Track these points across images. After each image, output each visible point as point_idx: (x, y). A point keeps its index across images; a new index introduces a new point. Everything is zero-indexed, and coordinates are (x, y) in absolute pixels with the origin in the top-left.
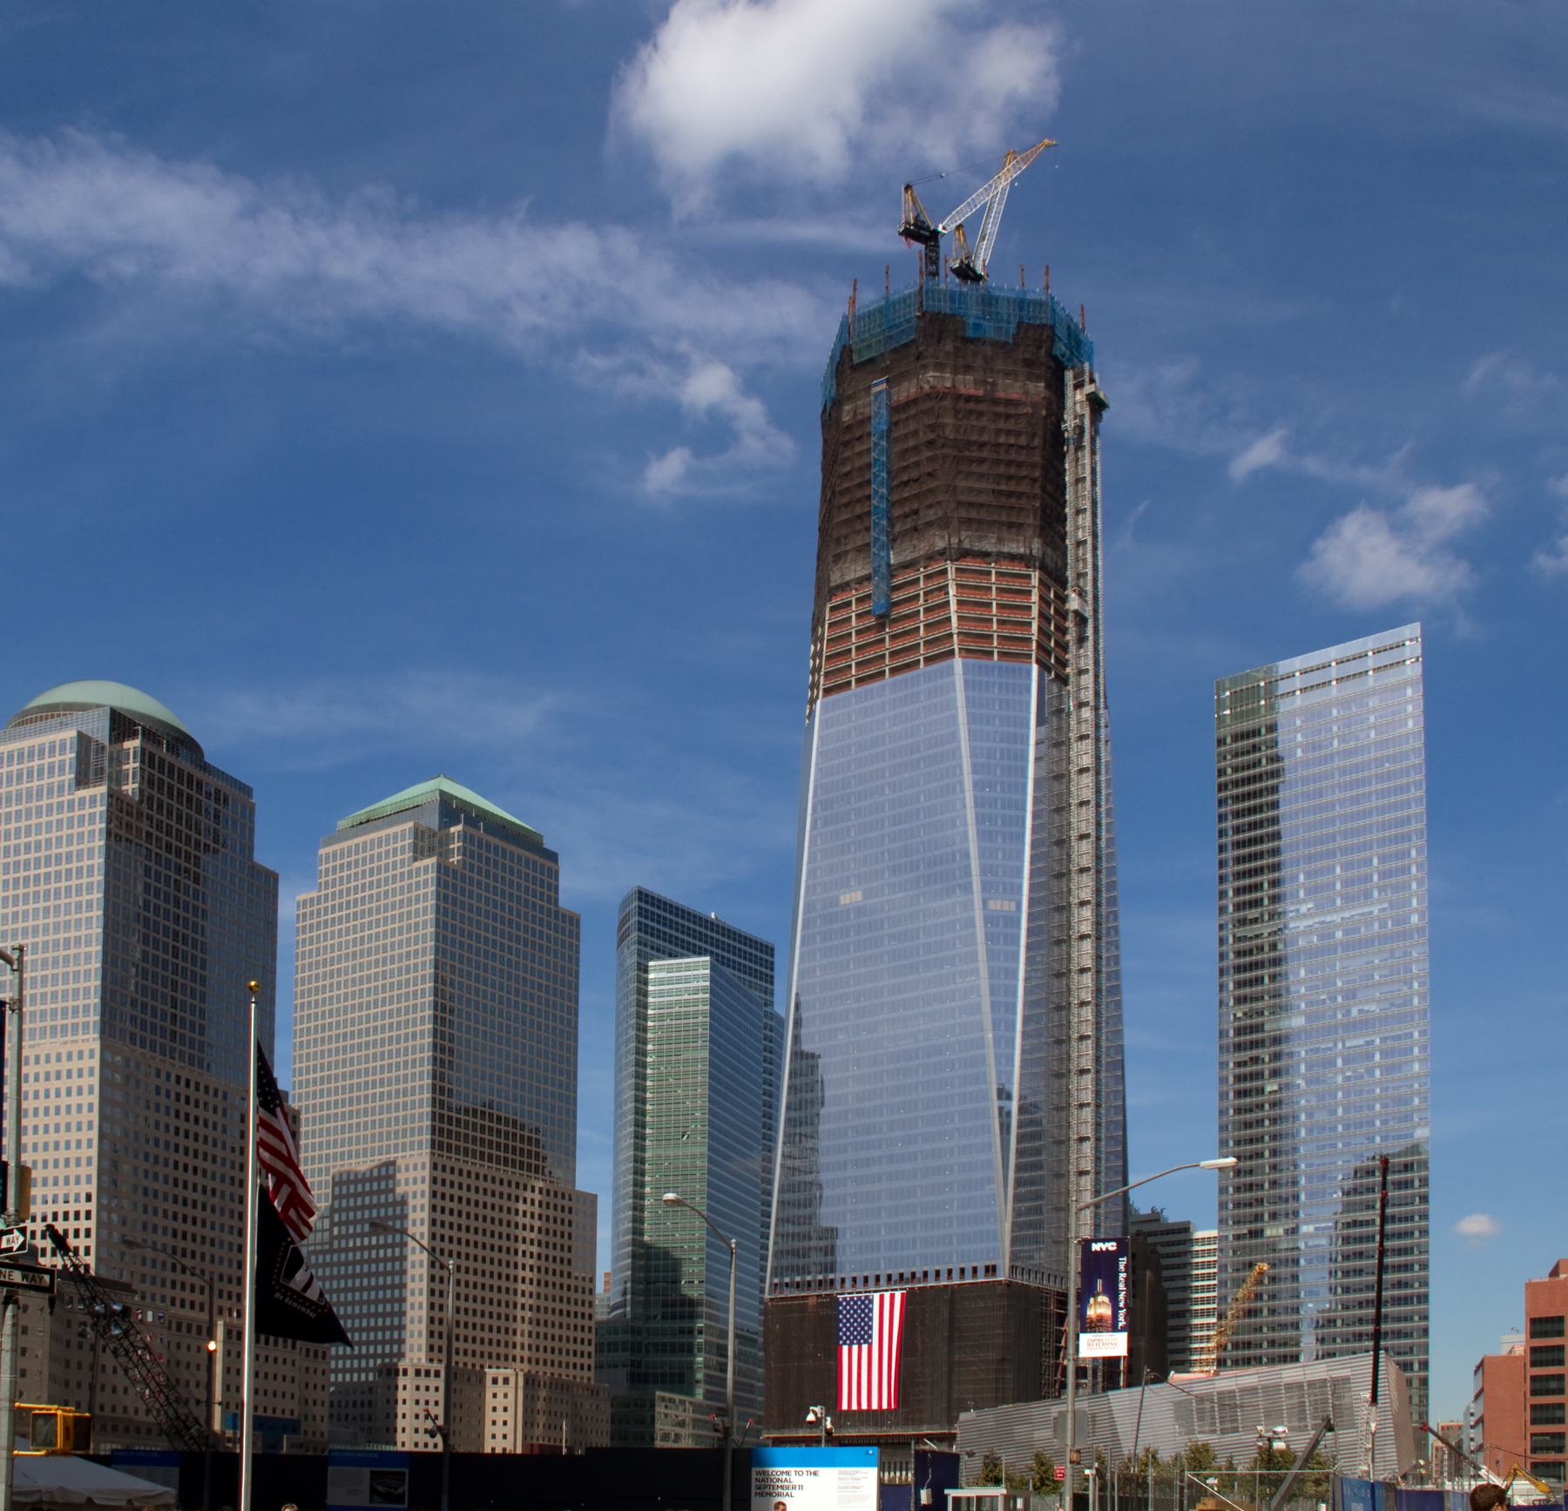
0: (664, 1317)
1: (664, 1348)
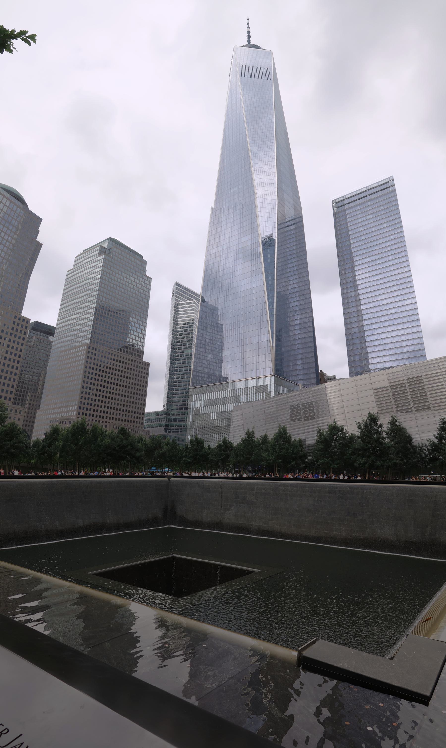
0: (177, 410)
1: (176, 420)
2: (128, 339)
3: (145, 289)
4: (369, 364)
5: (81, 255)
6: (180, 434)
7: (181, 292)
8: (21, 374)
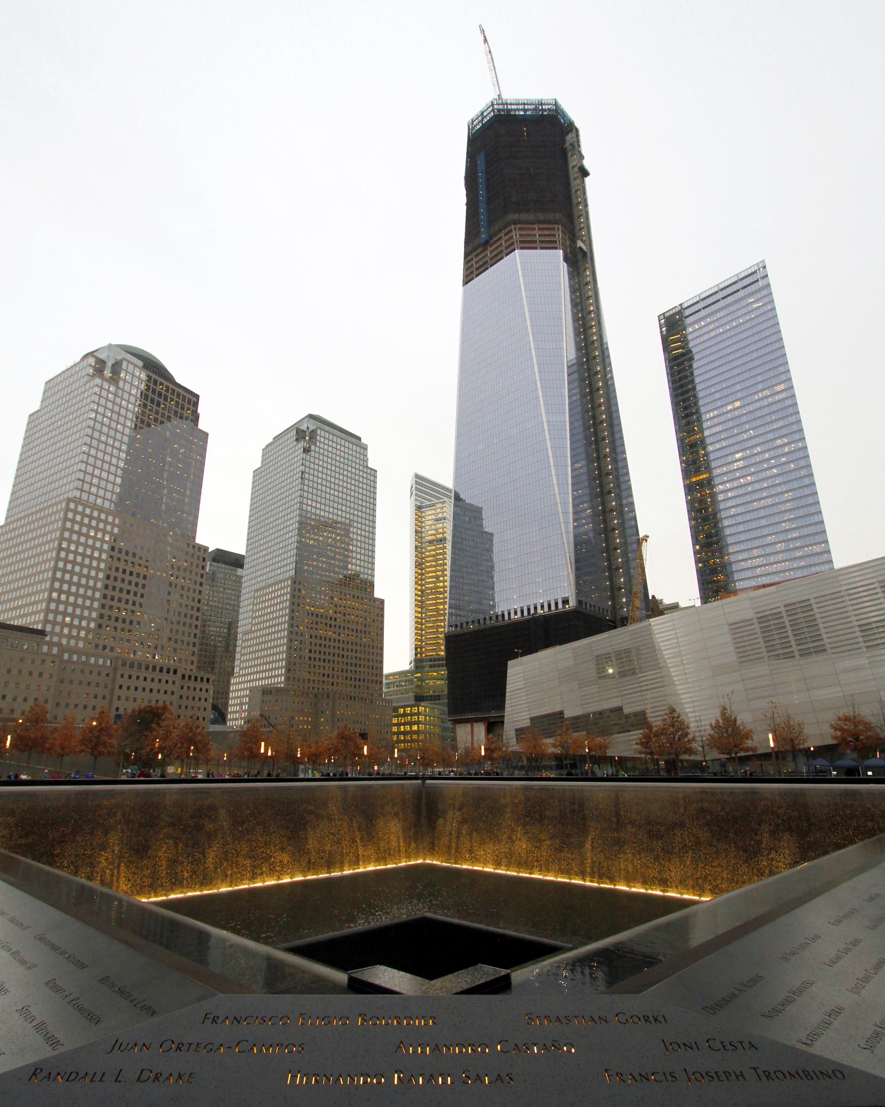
2: (350, 566)
3: (368, 488)
5: (271, 444)
6: (439, 704)
7: (424, 489)
8: (204, 626)
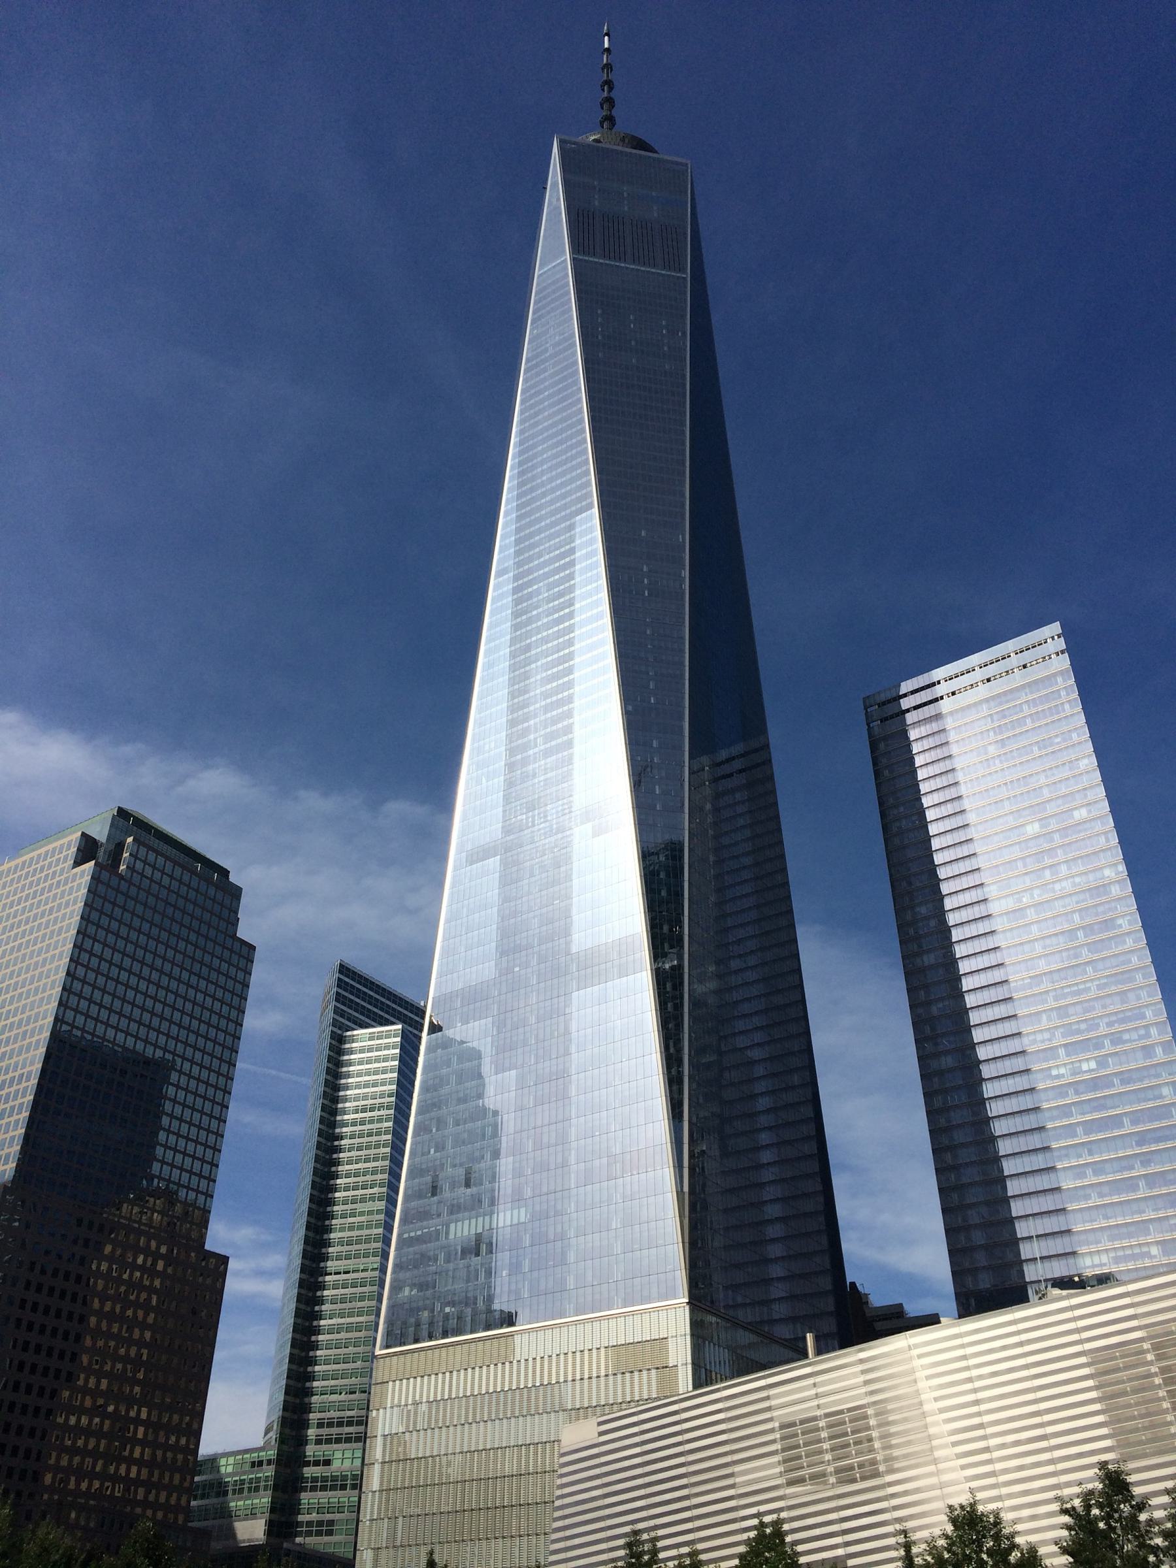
2: (156, 1167)
3: (230, 983)
4: (1021, 1262)
